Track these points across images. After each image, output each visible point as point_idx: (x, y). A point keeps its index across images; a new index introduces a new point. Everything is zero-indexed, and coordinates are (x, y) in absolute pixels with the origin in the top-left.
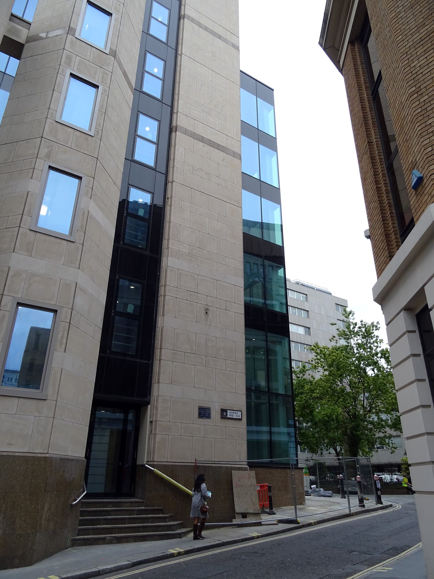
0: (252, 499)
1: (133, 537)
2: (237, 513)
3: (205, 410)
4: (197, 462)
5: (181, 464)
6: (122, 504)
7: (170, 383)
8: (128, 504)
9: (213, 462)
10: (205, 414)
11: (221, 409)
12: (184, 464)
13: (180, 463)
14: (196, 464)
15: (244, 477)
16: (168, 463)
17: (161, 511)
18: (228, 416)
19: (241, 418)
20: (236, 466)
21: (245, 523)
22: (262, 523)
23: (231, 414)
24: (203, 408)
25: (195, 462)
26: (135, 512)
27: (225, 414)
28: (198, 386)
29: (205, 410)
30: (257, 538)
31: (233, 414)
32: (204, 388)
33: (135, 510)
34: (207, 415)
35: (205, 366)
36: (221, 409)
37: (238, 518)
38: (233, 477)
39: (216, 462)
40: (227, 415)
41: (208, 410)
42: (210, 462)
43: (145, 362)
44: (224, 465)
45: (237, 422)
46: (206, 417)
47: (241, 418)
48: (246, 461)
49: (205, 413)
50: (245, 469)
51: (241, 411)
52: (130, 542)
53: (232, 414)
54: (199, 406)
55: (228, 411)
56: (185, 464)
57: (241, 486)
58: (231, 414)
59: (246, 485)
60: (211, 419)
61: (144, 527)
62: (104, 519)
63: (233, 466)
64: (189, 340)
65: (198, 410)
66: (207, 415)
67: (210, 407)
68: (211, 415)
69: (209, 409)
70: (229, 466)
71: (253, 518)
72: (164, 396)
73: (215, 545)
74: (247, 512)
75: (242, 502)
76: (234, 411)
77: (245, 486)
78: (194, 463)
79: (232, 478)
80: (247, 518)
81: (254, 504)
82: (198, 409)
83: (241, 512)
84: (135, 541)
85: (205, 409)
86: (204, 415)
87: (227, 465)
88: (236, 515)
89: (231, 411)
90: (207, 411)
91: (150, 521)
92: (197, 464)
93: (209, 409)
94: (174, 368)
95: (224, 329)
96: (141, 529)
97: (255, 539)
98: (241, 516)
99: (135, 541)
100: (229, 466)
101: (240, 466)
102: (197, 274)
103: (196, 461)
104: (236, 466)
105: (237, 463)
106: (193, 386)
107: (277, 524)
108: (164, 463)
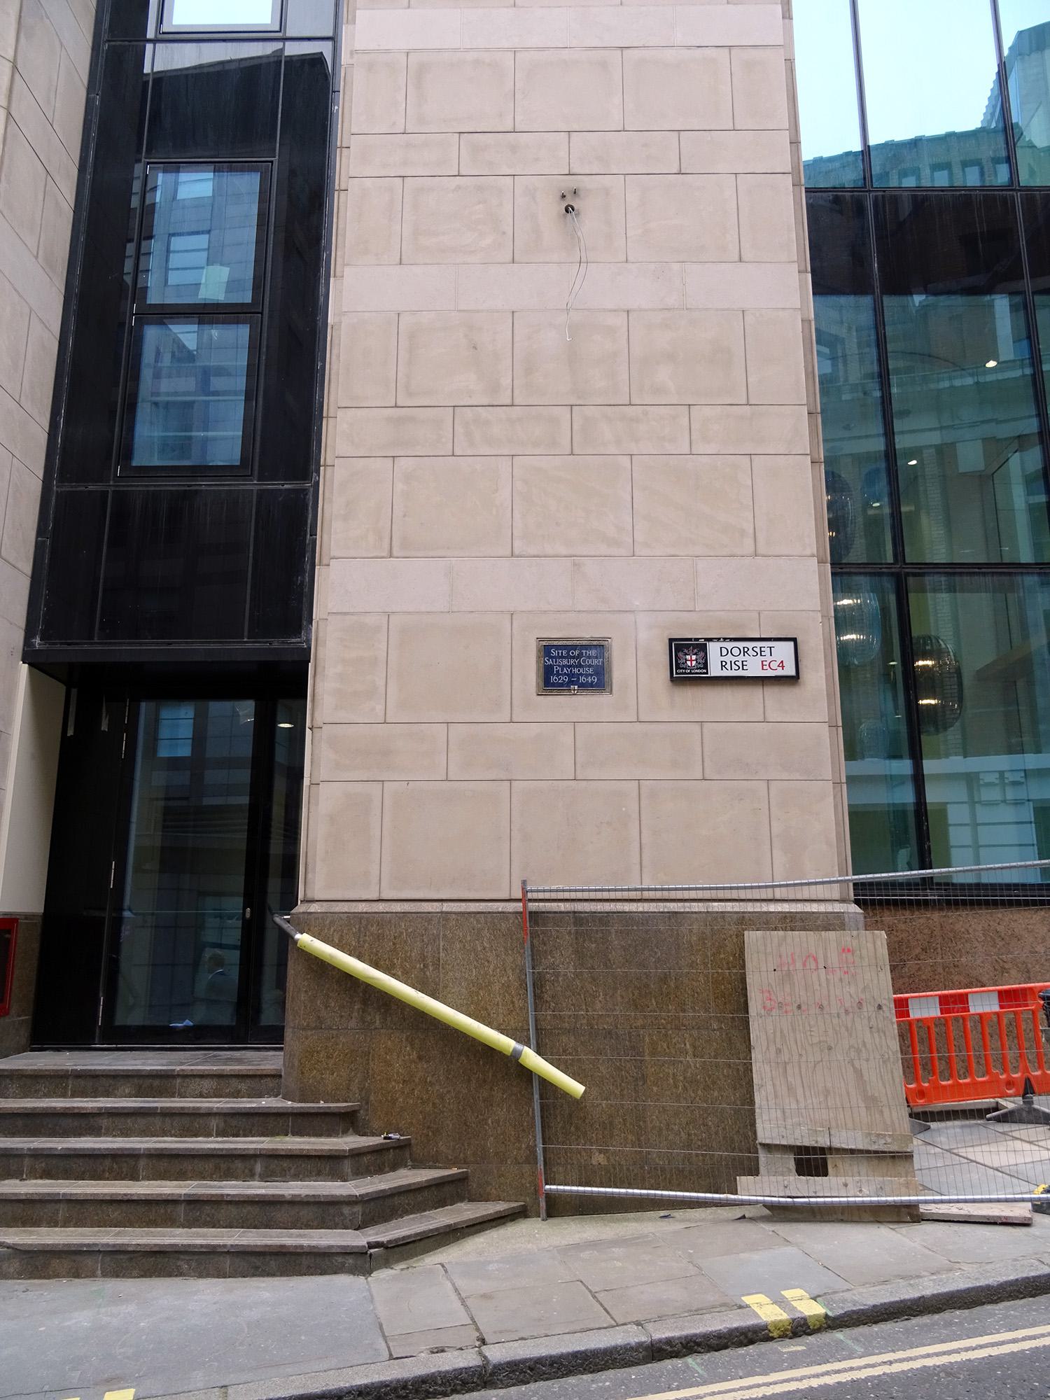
0: (859, 1074)
1: (105, 1252)
2: (768, 1147)
3: (576, 653)
4: (530, 896)
5: (447, 907)
6: (179, 1081)
7: (384, 554)
8: (207, 1084)
9: (633, 895)
10: (576, 670)
11: (671, 640)
12: (462, 910)
13: (445, 904)
14: (525, 907)
15: (815, 960)
16: (381, 907)
17: (348, 1121)
18: (715, 670)
19: (793, 673)
20: (772, 908)
21: (809, 1203)
22: (923, 1208)
23: (729, 658)
24: (565, 647)
25: (520, 896)
26: (214, 1123)
27: (691, 660)
28: (532, 550)
29: (576, 653)
30: (783, 1336)
31: (741, 658)
32: (564, 551)
33: (209, 1114)
34: (587, 676)
35: (572, 454)
36: (671, 640)
37: (769, 1174)
38: (749, 965)
39: (646, 895)
40: (705, 666)
41: (593, 653)
42: (619, 895)
43: (286, 486)
44: (696, 907)
45: (772, 692)
46: (584, 687)
47: (793, 673)
48: (837, 882)
49: (580, 666)
50: (832, 923)
51: (794, 640)
52: (92, 1275)
53: (734, 659)
54: (540, 640)
55: (713, 648)
56: (473, 907)
57: (799, 1007)
58: (729, 658)
59: (825, 1003)
60: (611, 692)
61: (194, 1202)
62: (36, 1155)
63: (750, 907)
64: (475, 348)
65: (538, 657)
66: (587, 676)
67: (605, 639)
68: (610, 671)
69: (600, 647)
70: (729, 907)
71: (864, 1178)
72: (352, 614)
73: (405, 1387)
74: (823, 1141)
75: (800, 1091)
76: (750, 645)
77: (821, 1007)
78: (530, 900)
79: (743, 967)
80: (826, 1175)
81: (871, 1102)
82: (539, 651)
83: (791, 1142)
84: (117, 1274)
85: (574, 647)
86: (571, 675)
87: (716, 907)
88: (763, 1157)
89: (729, 645)
90: (589, 657)
91: (258, 1168)
92: (530, 904)
93: (600, 647)
94: (400, 486)
95: (676, 267)
96: (181, 1209)
97: (769, 1339)
98: (792, 1165)
99: (117, 1272)
100: (729, 907)
101: (785, 907)
102: (508, 50)
103: (525, 892)
104: (772, 908)
105: (779, 893)
106: (508, 553)
107: (1025, 1224)
108: (362, 907)
